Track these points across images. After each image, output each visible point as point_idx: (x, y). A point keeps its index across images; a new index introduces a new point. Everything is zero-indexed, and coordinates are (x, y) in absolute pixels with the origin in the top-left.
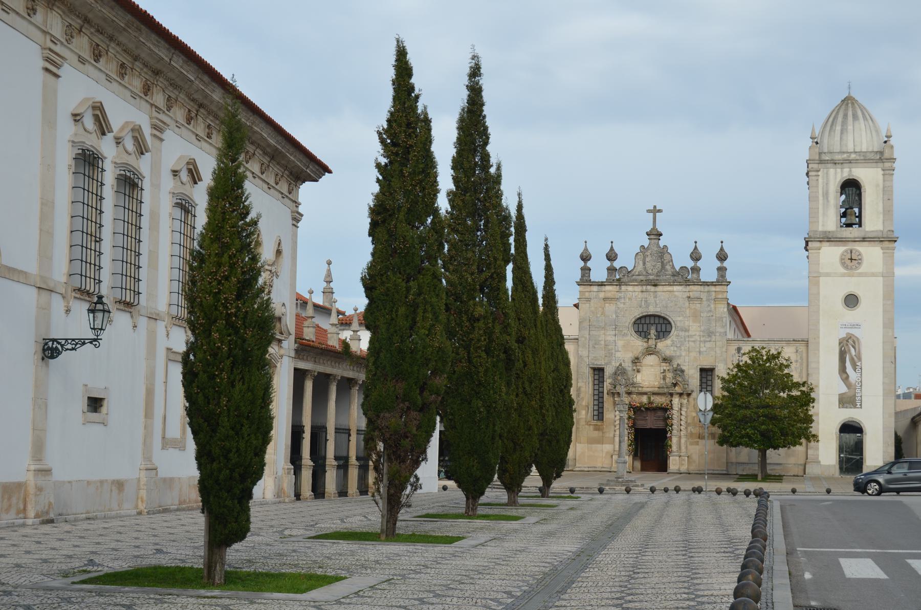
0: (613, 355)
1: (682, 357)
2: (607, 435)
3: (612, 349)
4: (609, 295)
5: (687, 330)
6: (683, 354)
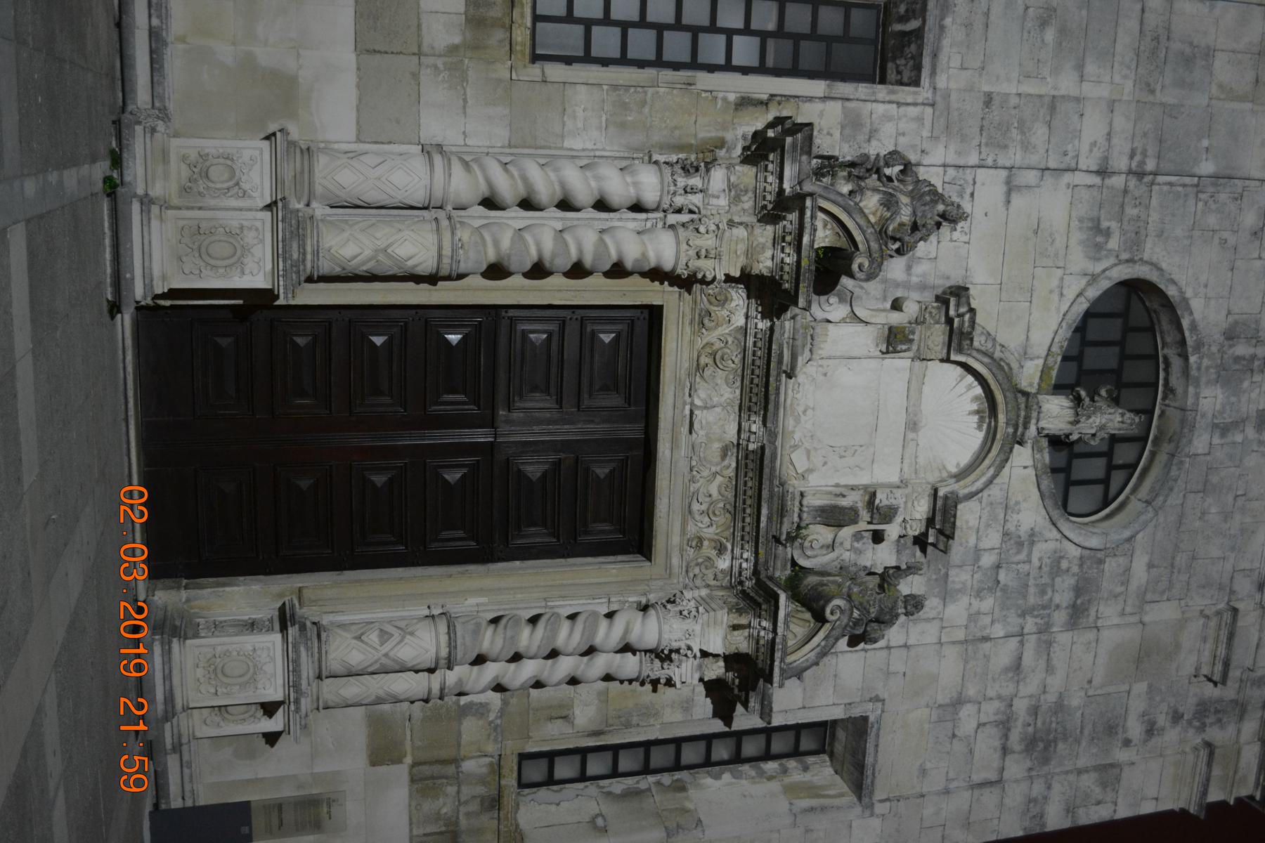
2: (435, 91)
3: (1026, 147)
5: (1077, 613)
6: (957, 611)
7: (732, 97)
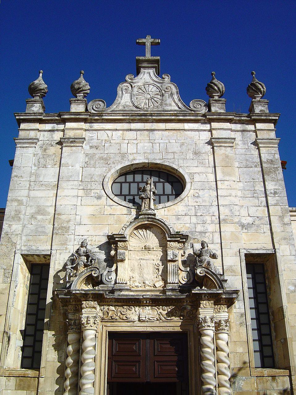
0: (71, 231)
1: (207, 234)
7: (52, 311)
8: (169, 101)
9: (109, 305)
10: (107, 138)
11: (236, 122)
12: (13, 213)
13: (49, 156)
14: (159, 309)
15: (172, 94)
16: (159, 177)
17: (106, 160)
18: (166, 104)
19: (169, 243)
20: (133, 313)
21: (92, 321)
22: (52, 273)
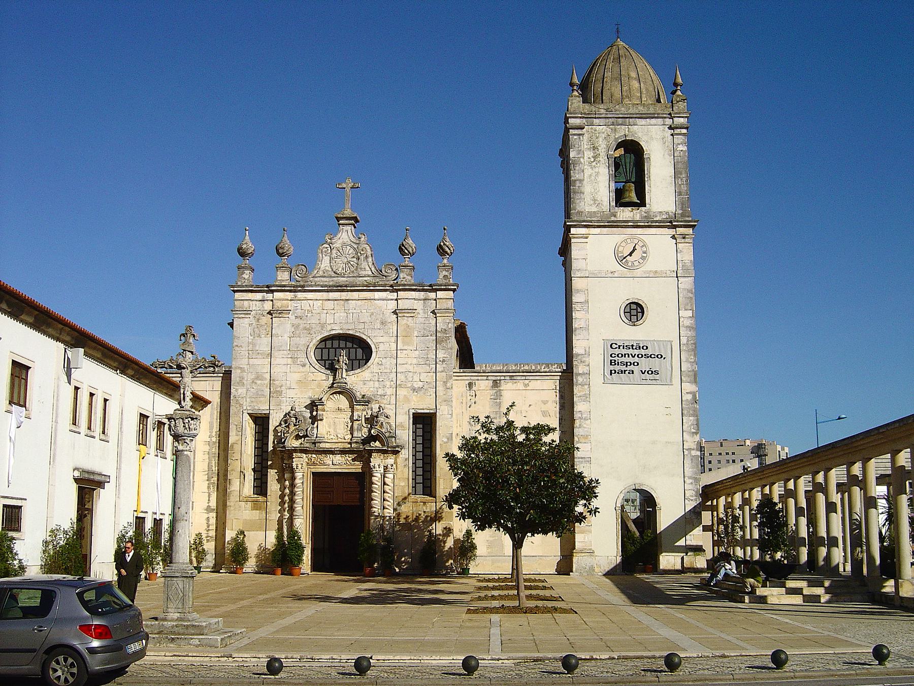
0: (284, 395)
1: (386, 397)
4: (278, 304)
8: (364, 265)
9: (312, 454)
10: (309, 308)
11: (419, 291)
12: (238, 379)
13: (262, 326)
14: (346, 456)
15: (367, 257)
16: (353, 343)
17: (308, 330)
18: (361, 269)
19: (355, 406)
20: (328, 459)
21: (300, 466)
22: (271, 428)
